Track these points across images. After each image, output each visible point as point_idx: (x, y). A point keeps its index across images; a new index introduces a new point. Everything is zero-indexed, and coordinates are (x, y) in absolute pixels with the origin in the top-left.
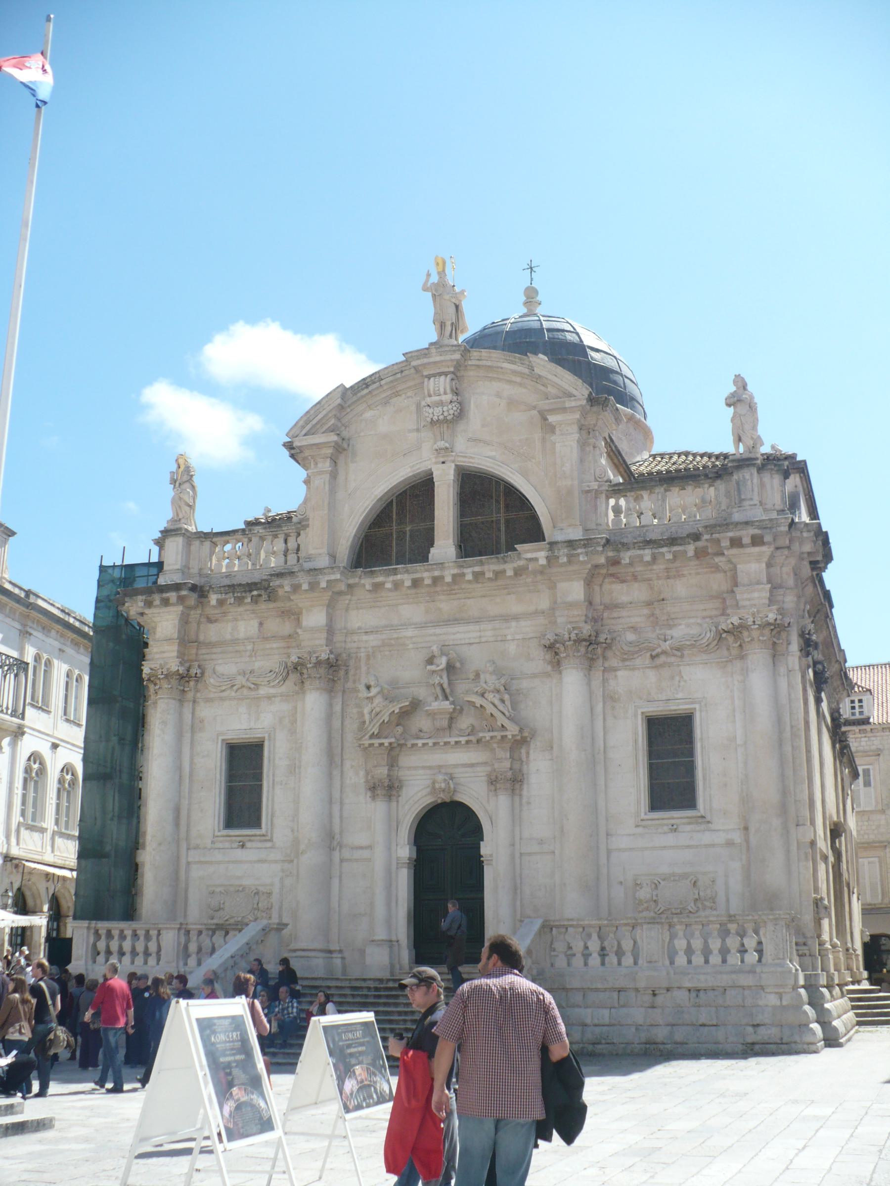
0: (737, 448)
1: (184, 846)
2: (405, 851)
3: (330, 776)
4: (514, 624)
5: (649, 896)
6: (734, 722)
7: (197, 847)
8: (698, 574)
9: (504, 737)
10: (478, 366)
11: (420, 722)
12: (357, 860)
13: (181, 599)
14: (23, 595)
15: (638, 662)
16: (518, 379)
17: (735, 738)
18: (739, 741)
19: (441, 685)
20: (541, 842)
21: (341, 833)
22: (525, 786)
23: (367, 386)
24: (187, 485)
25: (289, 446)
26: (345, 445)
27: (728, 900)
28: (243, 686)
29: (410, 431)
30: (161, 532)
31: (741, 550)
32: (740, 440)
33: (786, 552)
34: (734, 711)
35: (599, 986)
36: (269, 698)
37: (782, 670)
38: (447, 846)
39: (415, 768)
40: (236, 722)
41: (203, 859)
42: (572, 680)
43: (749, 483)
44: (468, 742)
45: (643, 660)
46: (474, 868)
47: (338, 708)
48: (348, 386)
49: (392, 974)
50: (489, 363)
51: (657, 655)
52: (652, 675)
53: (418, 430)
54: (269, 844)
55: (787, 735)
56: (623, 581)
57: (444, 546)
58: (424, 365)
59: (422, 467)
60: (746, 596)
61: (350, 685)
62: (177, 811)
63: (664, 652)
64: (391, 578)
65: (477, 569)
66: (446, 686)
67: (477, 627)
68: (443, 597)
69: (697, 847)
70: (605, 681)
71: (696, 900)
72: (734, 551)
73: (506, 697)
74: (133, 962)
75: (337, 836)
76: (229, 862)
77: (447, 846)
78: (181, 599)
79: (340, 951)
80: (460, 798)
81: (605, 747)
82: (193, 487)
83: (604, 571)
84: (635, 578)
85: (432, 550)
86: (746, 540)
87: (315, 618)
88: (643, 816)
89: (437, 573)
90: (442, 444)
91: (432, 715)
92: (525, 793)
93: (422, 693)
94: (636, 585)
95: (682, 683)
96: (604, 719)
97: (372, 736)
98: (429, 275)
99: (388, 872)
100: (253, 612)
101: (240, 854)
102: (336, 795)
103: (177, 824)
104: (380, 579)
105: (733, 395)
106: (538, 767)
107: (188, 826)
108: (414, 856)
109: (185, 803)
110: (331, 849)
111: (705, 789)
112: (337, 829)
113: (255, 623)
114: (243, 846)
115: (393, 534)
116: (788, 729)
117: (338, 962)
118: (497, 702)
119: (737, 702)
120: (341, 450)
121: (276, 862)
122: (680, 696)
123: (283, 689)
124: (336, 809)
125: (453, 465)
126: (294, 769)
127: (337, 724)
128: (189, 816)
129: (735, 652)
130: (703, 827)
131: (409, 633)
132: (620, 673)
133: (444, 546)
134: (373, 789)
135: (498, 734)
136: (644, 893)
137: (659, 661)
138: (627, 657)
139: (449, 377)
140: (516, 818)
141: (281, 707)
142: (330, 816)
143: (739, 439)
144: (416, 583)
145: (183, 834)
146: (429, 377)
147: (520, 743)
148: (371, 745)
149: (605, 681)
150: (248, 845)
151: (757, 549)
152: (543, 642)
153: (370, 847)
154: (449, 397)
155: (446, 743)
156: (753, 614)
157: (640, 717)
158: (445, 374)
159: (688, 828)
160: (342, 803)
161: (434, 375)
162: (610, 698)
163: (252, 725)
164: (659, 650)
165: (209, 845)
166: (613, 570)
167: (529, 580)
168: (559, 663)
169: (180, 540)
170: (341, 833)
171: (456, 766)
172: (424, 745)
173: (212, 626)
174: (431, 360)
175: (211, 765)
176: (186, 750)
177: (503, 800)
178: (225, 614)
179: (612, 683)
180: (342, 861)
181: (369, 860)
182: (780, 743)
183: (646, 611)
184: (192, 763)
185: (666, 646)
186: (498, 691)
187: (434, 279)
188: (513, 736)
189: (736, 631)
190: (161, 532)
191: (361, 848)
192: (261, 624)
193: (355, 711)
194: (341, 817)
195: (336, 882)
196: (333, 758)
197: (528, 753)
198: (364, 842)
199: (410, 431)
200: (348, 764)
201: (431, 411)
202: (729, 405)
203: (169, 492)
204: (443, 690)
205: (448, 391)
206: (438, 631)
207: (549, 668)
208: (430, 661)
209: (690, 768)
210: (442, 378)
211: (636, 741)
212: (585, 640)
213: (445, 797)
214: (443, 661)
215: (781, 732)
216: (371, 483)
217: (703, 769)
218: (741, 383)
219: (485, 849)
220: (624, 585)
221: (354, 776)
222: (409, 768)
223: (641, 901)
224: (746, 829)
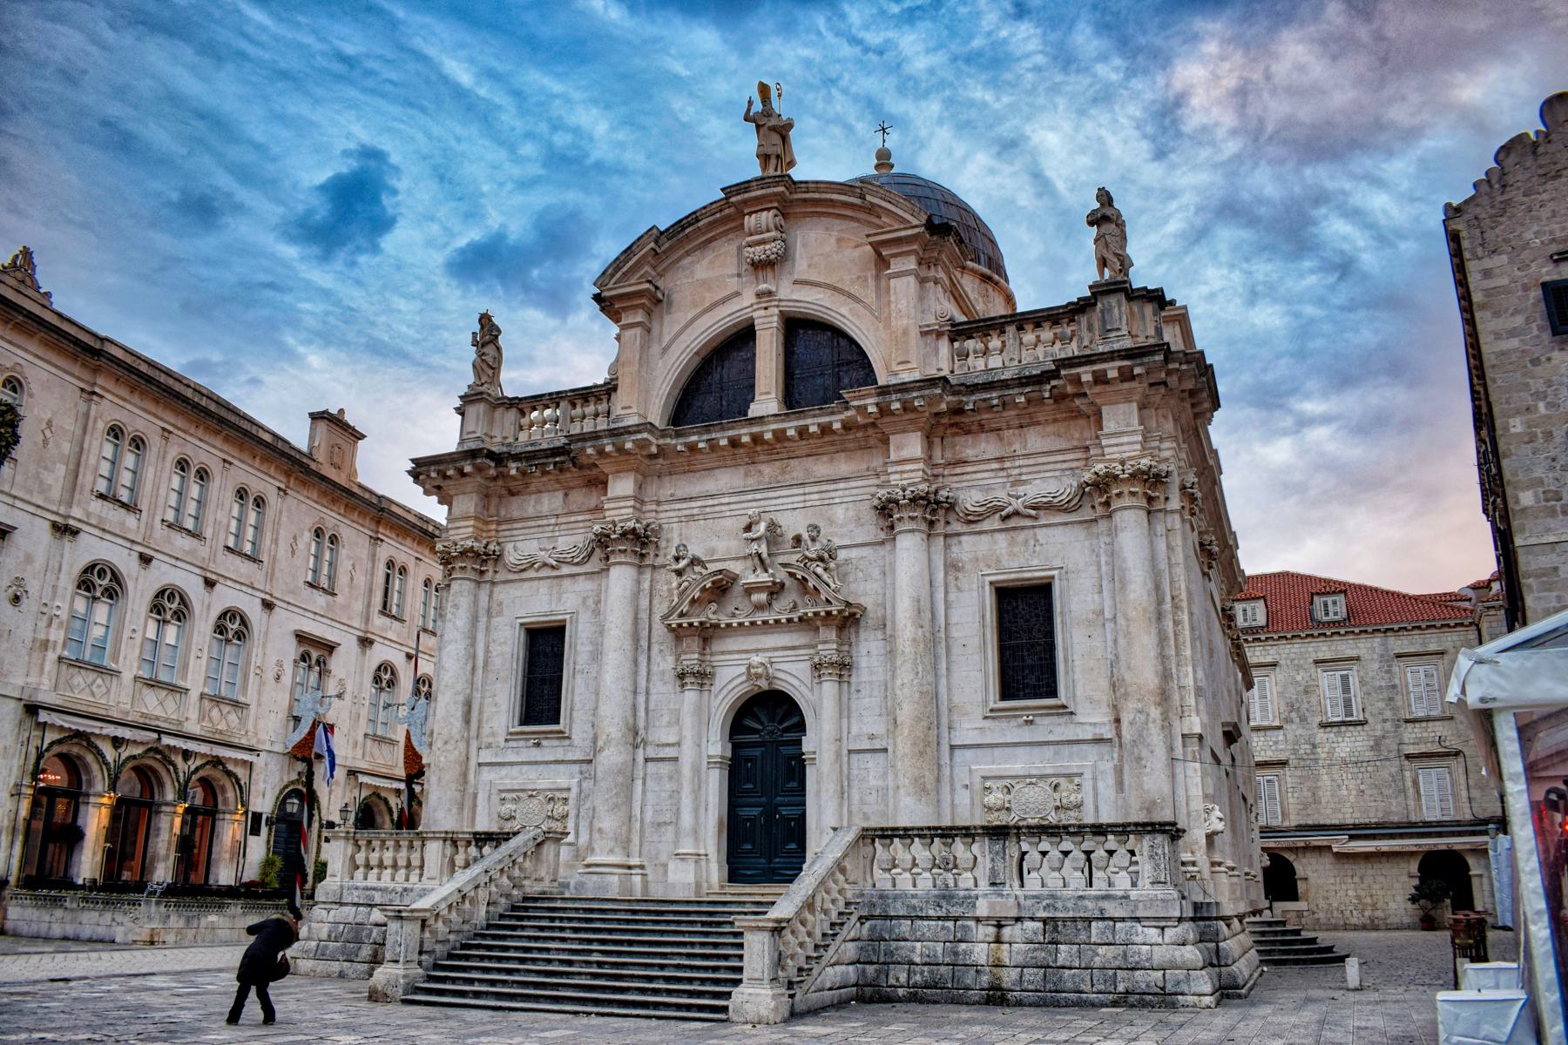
0: (1102, 274)
1: (474, 745)
2: (717, 746)
3: (636, 662)
4: (842, 485)
5: (999, 803)
6: (1100, 592)
7: (489, 746)
8: (1055, 421)
9: (829, 613)
10: (805, 200)
11: (736, 599)
12: (662, 759)
13: (479, 469)
14: (374, 500)
15: (986, 526)
16: (849, 213)
17: (1102, 612)
18: (1108, 615)
19: (759, 555)
20: (872, 737)
21: (646, 728)
22: (854, 672)
23: (684, 228)
24: (492, 346)
25: (598, 298)
26: (660, 295)
27: (1097, 808)
28: (545, 565)
29: (732, 276)
30: (461, 397)
31: (1108, 388)
32: (1105, 265)
33: (1162, 390)
34: (1101, 578)
35: (931, 913)
36: (572, 576)
37: (1160, 529)
38: (766, 745)
39: (730, 653)
40: (535, 602)
41: (494, 760)
42: (909, 547)
43: (1116, 311)
44: (789, 621)
45: (994, 523)
46: (795, 770)
47: (646, 585)
48: (662, 229)
49: (698, 893)
50: (816, 196)
51: (1008, 517)
52: (1000, 537)
53: (739, 275)
54: (567, 742)
55: (1168, 606)
56: (968, 432)
57: (766, 401)
58: (745, 202)
59: (744, 315)
60: (1113, 441)
62: (468, 705)
63: (1017, 513)
64: (705, 437)
65: (801, 423)
66: (765, 556)
67: (801, 491)
68: (762, 458)
69: (1058, 743)
70: (947, 547)
71: (1057, 808)
72: (1098, 389)
73: (832, 565)
74: (366, 878)
75: (642, 732)
76: (522, 763)
77: (766, 745)
78: (479, 469)
79: (642, 867)
80: (780, 686)
81: (947, 624)
82: (498, 349)
83: (945, 421)
84: (982, 428)
85: (752, 406)
86: (1113, 374)
87: (622, 486)
88: (992, 705)
89: (755, 429)
90: (763, 287)
91: (749, 590)
92: (853, 679)
93: (735, 567)
95: (1038, 548)
96: (946, 593)
97: (682, 615)
98: (750, 103)
99: (696, 770)
100: (558, 481)
101: (536, 754)
102: (642, 683)
103: (467, 721)
104: (694, 438)
105: (1094, 212)
106: (868, 649)
107: (480, 722)
108: (729, 754)
109: (477, 695)
110: (636, 747)
111: (1067, 673)
112: (641, 724)
113: (560, 495)
114: (538, 745)
115: (711, 387)
116: (1168, 599)
117: (637, 879)
118: (819, 570)
119: (1104, 568)
120: (655, 302)
121: (575, 762)
122: (1035, 562)
124: (641, 699)
125: (776, 311)
126: (597, 655)
127: (644, 603)
128: (481, 713)
129: (1100, 510)
130: (1066, 718)
131: (726, 500)
132: (964, 539)
133: (766, 401)
134: (681, 676)
135: (822, 610)
136: (991, 799)
137: (1012, 523)
138: (972, 519)
139: (772, 212)
140: (844, 710)
141: (584, 585)
142: (634, 707)
143: (1103, 263)
144: (734, 443)
145: (473, 733)
146: (750, 214)
147: (848, 620)
148: (680, 625)
149: (947, 547)
150: (544, 743)
151: (1126, 385)
152: (876, 502)
153: (678, 744)
155: (765, 623)
156: (1123, 463)
157: (987, 588)
158: (768, 209)
159: (1047, 720)
160: (647, 693)
162: (952, 567)
163: (553, 607)
164: (1010, 509)
165: (502, 744)
166: (958, 419)
167: (860, 434)
168: (892, 527)
169: (481, 407)
170: (646, 728)
171: (775, 649)
172: (741, 624)
174: (753, 194)
175: (507, 651)
176: (481, 636)
177: (829, 688)
178: (527, 485)
179: (955, 549)
180: (647, 760)
181: (676, 759)
182: (1160, 616)
183: (995, 466)
184: (487, 651)
185: (1017, 505)
186: (821, 559)
187: (758, 107)
188: (840, 612)
189: (1102, 485)
190: (461, 397)
191: (668, 745)
192: (566, 495)
194: (647, 709)
195: (639, 783)
196: (638, 641)
197: (857, 632)
198: (672, 740)
199: (732, 276)
200: (655, 648)
202: (1091, 224)
203: (471, 353)
204: (762, 561)
205: (772, 226)
206: (758, 496)
207: (882, 535)
208: (748, 528)
209: (1051, 648)
211: (983, 617)
212: (922, 498)
213: (764, 685)
214: (762, 528)
215: (1160, 602)
216: (687, 334)
217: (1065, 649)
218: (1105, 197)
219: (808, 745)
220: (969, 438)
221: (665, 663)
222: (723, 653)
223: (990, 809)
224: (1118, 721)
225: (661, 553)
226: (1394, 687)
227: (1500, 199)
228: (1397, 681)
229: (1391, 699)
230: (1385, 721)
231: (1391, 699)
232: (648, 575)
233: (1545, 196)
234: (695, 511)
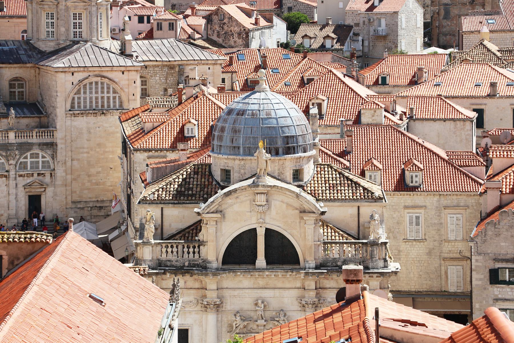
29: (247, 212)
43: (375, 252)
53: (251, 212)
57: (261, 261)
61: (224, 309)
94: (332, 281)
123: (196, 309)
154: (265, 203)
161: (259, 193)
173: (164, 281)
192: (185, 282)
193: (226, 319)
199: (247, 212)
201: (258, 208)
207: (300, 309)
210: (263, 195)
220: (328, 281)
225: (224, 307)
226: (441, 224)
227: (484, 238)
228: (443, 221)
229: (439, 230)
230: (435, 241)
231: (439, 230)
232: (220, 316)
233: (495, 241)
234: (236, 294)
